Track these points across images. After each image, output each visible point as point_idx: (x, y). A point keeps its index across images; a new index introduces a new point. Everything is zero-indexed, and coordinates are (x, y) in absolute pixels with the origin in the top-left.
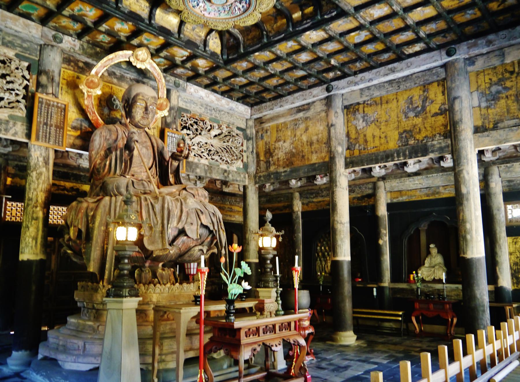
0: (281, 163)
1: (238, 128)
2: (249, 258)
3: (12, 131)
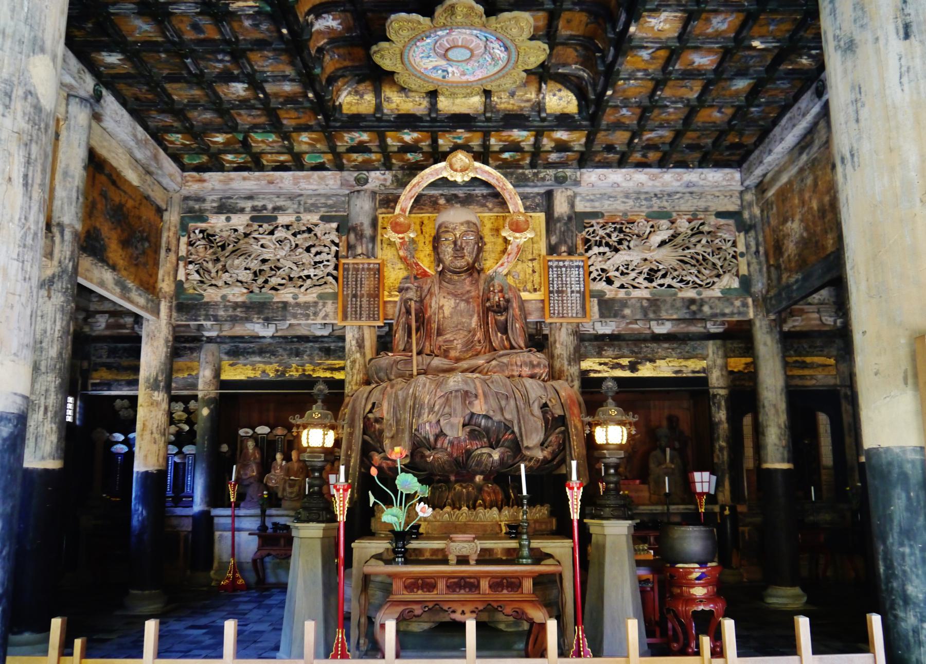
0: (793, 265)
1: (720, 215)
2: (766, 462)
3: (322, 314)
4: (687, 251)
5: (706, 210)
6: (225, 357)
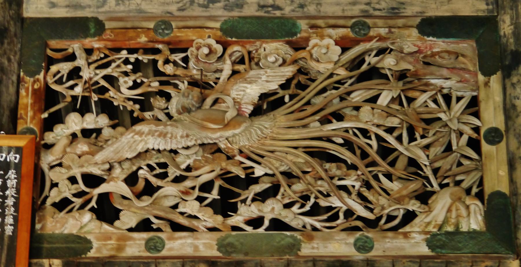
1: (431, 26)
4: (336, 125)
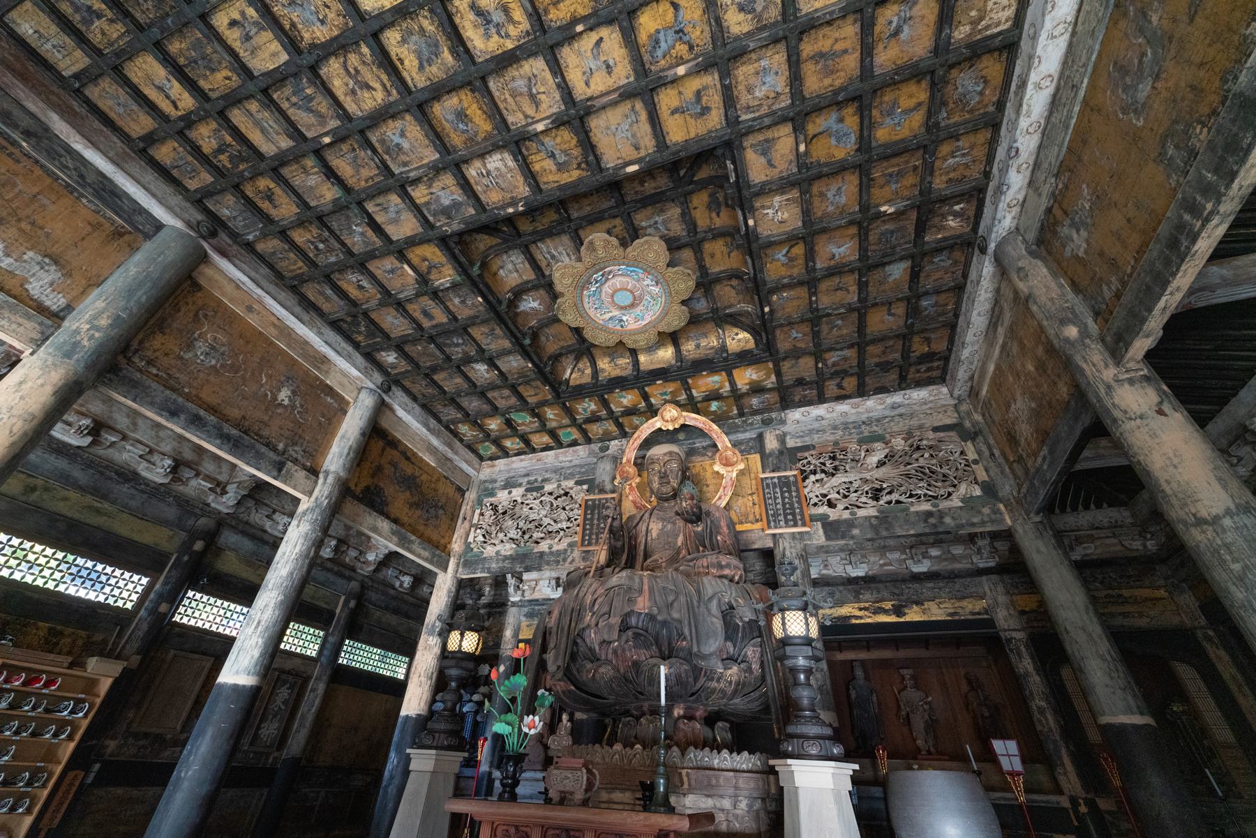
3: (570, 559)
5: (921, 427)
6: (523, 619)
